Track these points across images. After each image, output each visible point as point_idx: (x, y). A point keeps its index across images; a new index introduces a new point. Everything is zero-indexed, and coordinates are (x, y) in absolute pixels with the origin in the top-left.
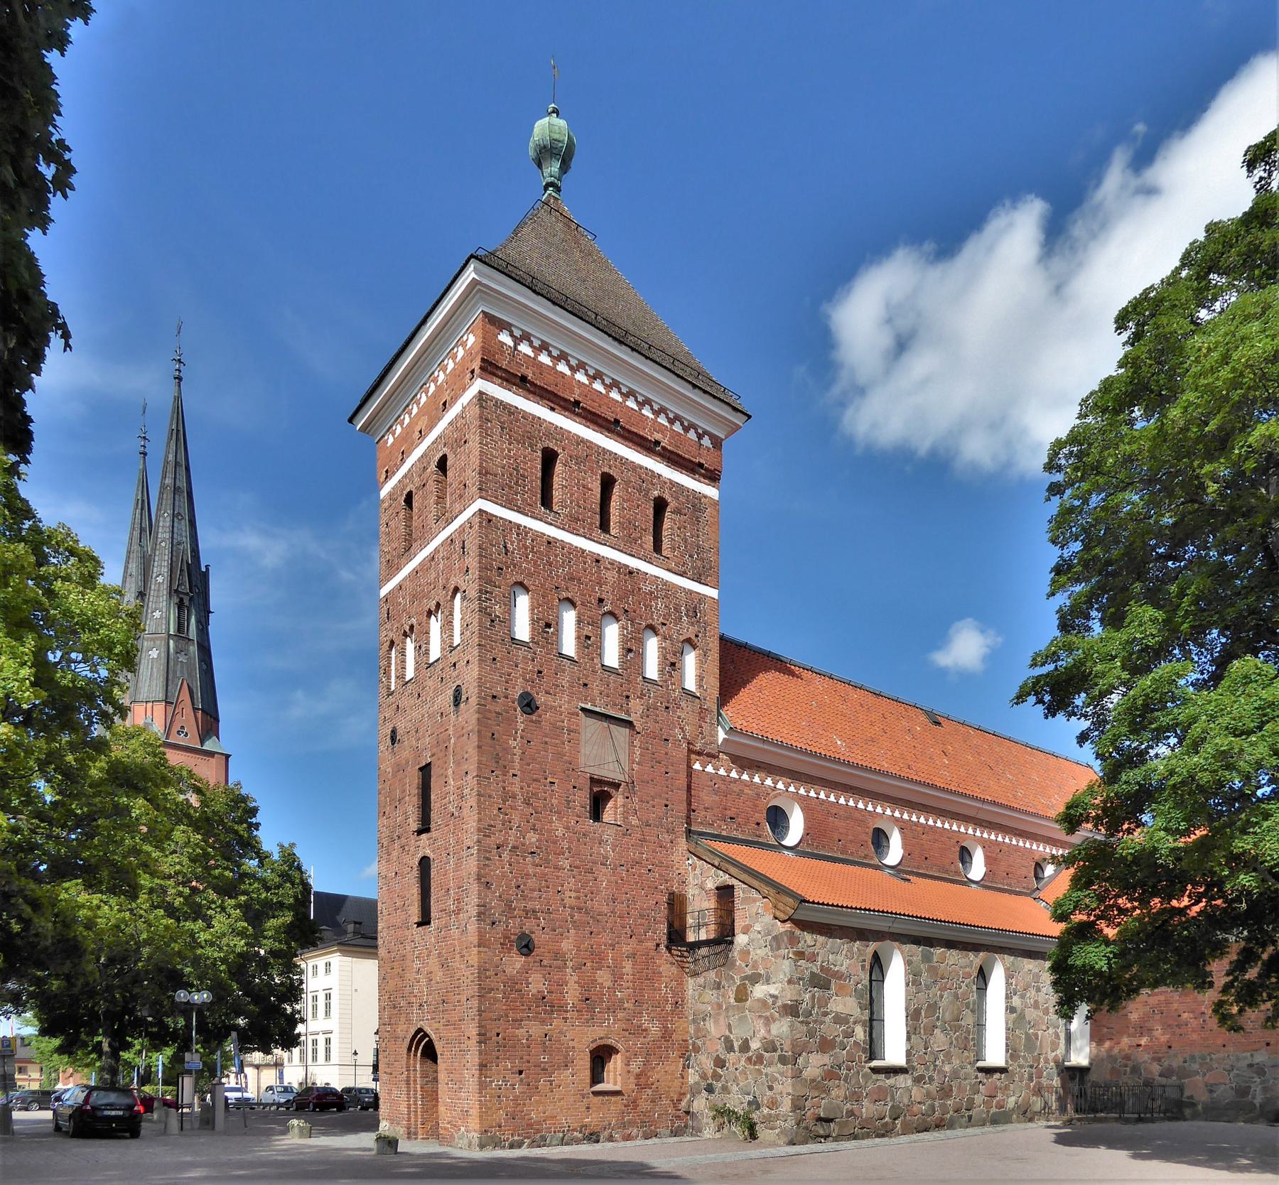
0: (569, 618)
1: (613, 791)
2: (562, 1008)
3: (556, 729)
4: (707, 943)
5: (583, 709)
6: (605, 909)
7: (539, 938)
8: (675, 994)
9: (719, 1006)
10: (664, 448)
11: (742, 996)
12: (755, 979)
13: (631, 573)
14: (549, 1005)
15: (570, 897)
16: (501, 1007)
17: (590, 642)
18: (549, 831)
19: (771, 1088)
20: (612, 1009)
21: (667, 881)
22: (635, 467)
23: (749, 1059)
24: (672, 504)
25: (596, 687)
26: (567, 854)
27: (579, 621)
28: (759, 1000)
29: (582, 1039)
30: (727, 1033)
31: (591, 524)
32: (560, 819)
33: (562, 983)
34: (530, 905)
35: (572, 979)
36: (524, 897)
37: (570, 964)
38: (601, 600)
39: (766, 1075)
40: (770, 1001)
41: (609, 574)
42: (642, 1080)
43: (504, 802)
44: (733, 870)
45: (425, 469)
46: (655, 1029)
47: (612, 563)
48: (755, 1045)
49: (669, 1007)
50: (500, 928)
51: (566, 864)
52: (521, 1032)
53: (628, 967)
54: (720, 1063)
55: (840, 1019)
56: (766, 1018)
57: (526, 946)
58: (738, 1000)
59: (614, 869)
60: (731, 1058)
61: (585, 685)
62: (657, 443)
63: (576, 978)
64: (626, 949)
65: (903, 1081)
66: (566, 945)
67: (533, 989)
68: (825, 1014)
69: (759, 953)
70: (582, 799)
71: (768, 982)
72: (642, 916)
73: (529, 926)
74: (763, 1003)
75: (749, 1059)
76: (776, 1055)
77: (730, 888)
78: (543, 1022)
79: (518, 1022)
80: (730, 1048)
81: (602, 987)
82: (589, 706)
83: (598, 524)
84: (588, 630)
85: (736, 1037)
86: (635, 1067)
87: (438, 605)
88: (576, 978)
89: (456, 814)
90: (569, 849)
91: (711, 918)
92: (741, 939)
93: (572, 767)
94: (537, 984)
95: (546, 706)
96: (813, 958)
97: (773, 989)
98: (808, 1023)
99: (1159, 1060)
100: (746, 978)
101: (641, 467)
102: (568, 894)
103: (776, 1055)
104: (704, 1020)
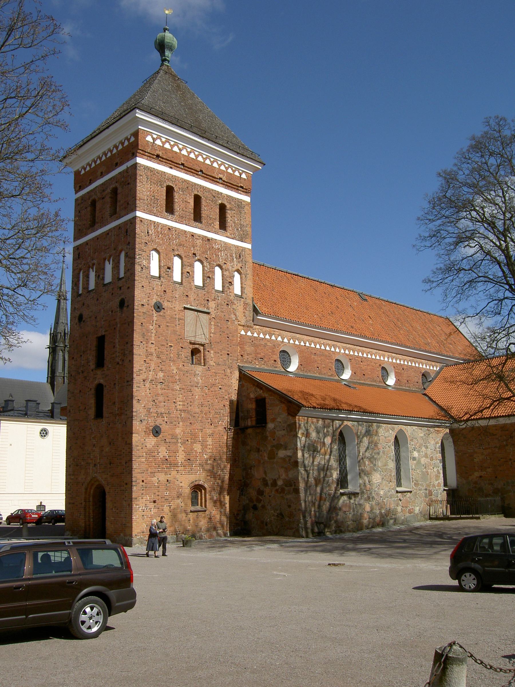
0: (177, 262)
1: (201, 348)
2: (176, 465)
4: (252, 427)
5: (185, 308)
6: (197, 410)
7: (164, 427)
10: (224, 181)
11: (272, 456)
12: (279, 447)
13: (209, 240)
14: (169, 463)
16: (144, 466)
18: (169, 371)
23: (277, 490)
24: (228, 206)
25: (192, 297)
26: (178, 382)
28: (281, 458)
30: (264, 476)
31: (189, 219)
32: (174, 364)
35: (181, 449)
36: (157, 406)
37: (180, 441)
38: (194, 254)
39: (287, 499)
40: (287, 459)
41: (198, 241)
43: (147, 357)
45: (104, 191)
47: (199, 236)
48: (280, 483)
50: (144, 423)
53: (210, 441)
56: (286, 468)
57: (156, 432)
58: (269, 458)
60: (267, 490)
61: (187, 296)
62: (220, 179)
63: (183, 449)
64: (209, 431)
66: (178, 431)
67: (161, 455)
71: (286, 448)
73: (159, 421)
74: (284, 459)
75: (277, 490)
76: (292, 488)
78: (166, 474)
82: (188, 306)
83: (192, 218)
84: (188, 269)
85: (270, 478)
88: (183, 449)
89: (121, 363)
91: (253, 414)
92: (270, 426)
93: (182, 338)
94: (163, 452)
95: (167, 308)
100: (274, 446)
101: (213, 190)
102: (179, 403)
103: (292, 488)
104: (251, 469)
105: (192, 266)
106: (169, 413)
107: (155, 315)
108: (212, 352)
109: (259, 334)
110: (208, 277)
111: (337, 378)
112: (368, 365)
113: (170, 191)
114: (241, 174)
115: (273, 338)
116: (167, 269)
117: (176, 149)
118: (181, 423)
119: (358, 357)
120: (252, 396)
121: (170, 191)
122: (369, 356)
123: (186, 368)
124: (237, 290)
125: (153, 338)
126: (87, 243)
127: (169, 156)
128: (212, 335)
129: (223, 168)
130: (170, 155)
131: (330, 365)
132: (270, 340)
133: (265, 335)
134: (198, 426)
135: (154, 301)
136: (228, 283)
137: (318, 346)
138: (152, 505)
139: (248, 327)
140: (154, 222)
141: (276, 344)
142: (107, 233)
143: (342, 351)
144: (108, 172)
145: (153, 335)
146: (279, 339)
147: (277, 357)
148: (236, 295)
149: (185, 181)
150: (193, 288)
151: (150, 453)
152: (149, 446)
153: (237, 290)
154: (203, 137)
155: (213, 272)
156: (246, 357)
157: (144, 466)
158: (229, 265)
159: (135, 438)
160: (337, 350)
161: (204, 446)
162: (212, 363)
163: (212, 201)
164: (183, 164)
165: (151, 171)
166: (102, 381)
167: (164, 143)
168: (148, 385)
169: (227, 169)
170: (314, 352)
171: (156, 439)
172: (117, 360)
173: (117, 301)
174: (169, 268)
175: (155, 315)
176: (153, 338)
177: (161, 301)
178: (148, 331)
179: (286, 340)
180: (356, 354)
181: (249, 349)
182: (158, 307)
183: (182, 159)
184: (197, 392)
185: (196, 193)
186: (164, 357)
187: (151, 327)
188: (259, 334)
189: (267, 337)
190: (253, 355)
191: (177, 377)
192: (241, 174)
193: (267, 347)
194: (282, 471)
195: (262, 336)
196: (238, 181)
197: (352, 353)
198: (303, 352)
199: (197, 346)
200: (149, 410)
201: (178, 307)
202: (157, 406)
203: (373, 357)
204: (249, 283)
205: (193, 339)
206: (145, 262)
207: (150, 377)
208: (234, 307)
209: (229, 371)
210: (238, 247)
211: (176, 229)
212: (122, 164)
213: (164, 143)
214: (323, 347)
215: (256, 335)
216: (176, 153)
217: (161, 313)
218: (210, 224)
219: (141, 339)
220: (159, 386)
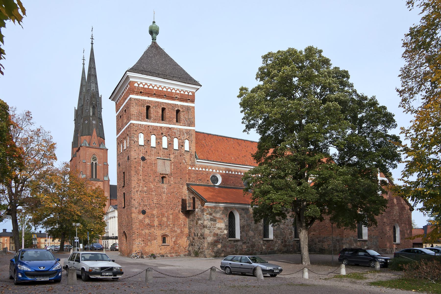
1: (167, 176)
2: (153, 226)
3: (151, 164)
6: (164, 203)
7: (147, 211)
8: (184, 222)
11: (197, 223)
12: (199, 219)
14: (150, 226)
15: (155, 201)
16: (138, 227)
17: (159, 143)
20: (167, 226)
22: (170, 104)
25: (161, 153)
32: (152, 184)
35: (156, 220)
42: (176, 243)
46: (179, 231)
48: (199, 235)
49: (182, 226)
50: (138, 209)
52: (143, 232)
53: (171, 217)
54: (194, 239)
57: (144, 212)
59: (167, 194)
65: (239, 243)
66: (155, 212)
69: (199, 213)
70: (159, 178)
73: (145, 208)
78: (149, 230)
79: (142, 230)
82: (159, 158)
86: (173, 240)
92: (197, 210)
93: (155, 172)
94: (147, 221)
99: (318, 238)
105: (161, 139)
109: (199, 169)
110: (170, 144)
114: (188, 93)
115: (207, 170)
118: (156, 209)
120: (191, 197)
121: (148, 108)
123: (158, 185)
132: (205, 171)
134: (164, 210)
135: (141, 156)
136: (181, 145)
138: (142, 242)
141: (208, 173)
145: (141, 171)
148: (186, 151)
150: (162, 149)
151: (141, 222)
155: (173, 141)
157: (138, 227)
158: (182, 137)
159: (133, 215)
161: (168, 219)
162: (172, 183)
168: (139, 193)
174: (148, 141)
178: (138, 170)
179: (214, 171)
181: (193, 175)
182: (143, 159)
184: (164, 196)
185: (163, 107)
186: (147, 181)
187: (140, 168)
188: (199, 169)
189: (204, 169)
191: (154, 189)
192: (188, 93)
195: (200, 169)
198: (222, 175)
199: (164, 176)
200: (140, 204)
202: (144, 202)
204: (194, 144)
205: (162, 172)
208: (184, 156)
209: (181, 186)
215: (197, 169)
217: (145, 162)
220: (145, 193)
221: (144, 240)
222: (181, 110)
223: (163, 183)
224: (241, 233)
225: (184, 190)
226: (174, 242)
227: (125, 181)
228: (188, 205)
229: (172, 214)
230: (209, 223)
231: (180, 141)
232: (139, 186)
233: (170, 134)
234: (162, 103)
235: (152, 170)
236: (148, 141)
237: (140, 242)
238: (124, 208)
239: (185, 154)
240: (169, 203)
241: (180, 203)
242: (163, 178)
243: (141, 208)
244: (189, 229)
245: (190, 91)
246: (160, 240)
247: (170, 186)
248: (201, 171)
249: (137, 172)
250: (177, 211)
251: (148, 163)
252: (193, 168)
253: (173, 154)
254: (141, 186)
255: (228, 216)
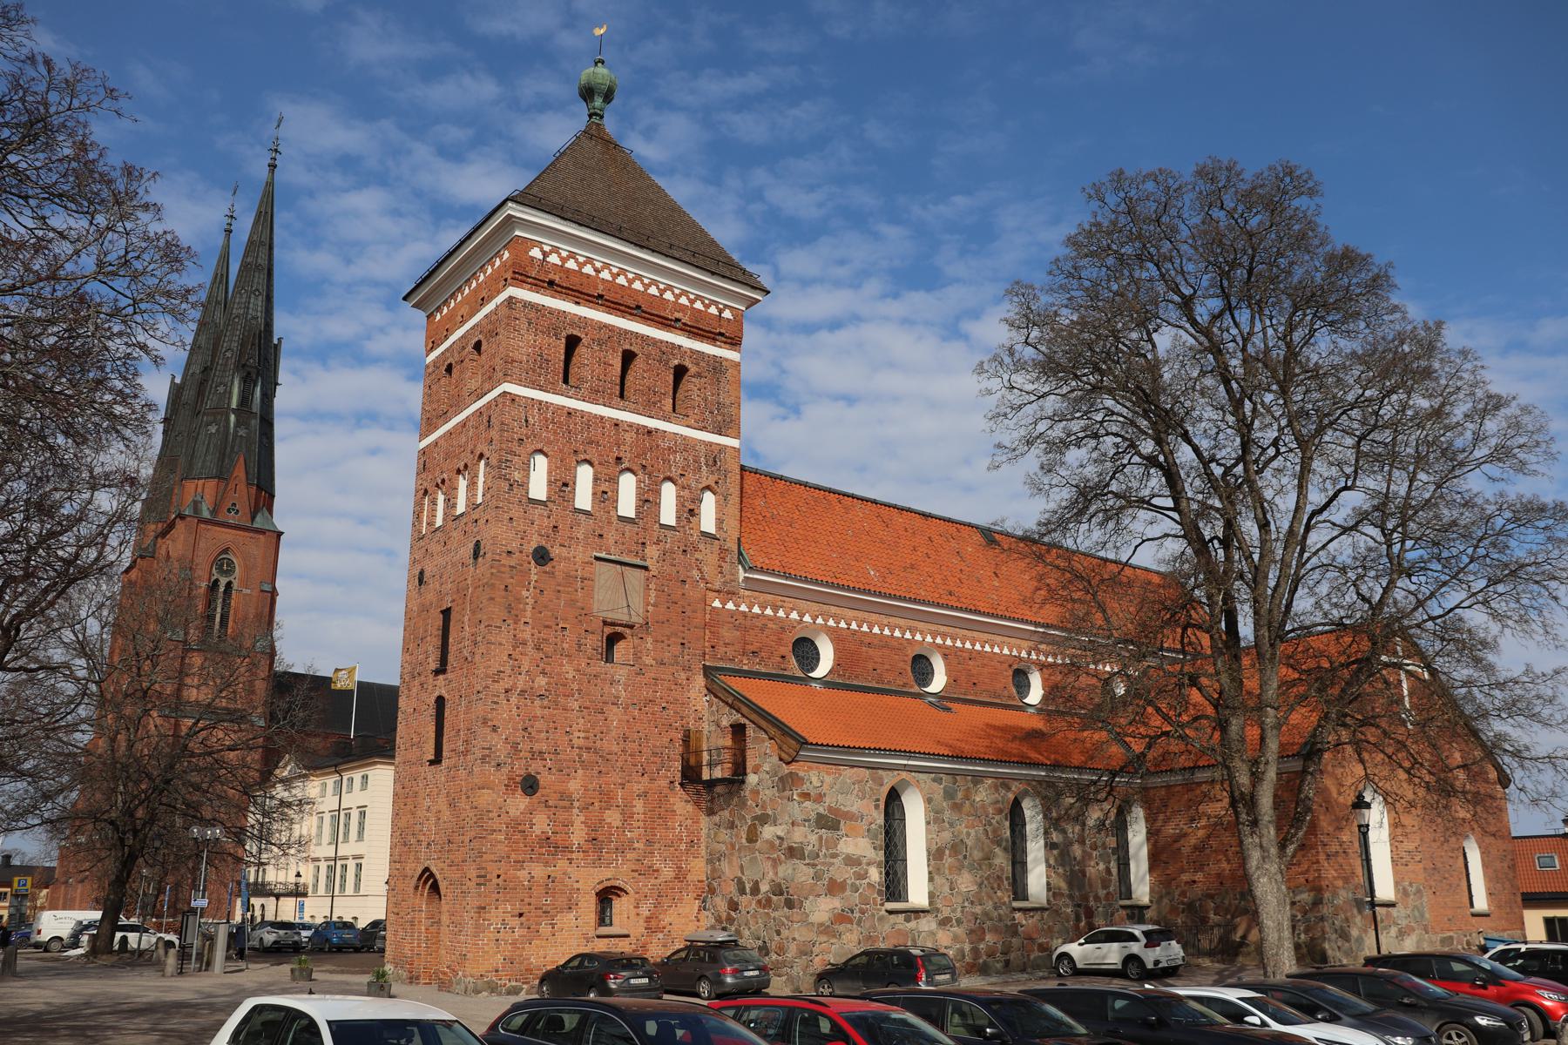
0: (585, 475)
2: (567, 849)
5: (597, 559)
6: (615, 748)
7: (545, 779)
8: (690, 833)
9: (733, 846)
11: (752, 837)
12: (763, 819)
13: (649, 432)
14: (553, 846)
16: (502, 849)
17: (605, 495)
19: (778, 933)
21: (682, 718)
27: (596, 479)
29: (588, 879)
32: (570, 662)
33: (567, 824)
34: (537, 747)
35: (578, 819)
36: (531, 738)
37: (576, 804)
38: (618, 459)
41: (627, 436)
42: (653, 923)
44: (745, 710)
46: (667, 872)
47: (631, 425)
48: (764, 888)
49: (683, 847)
50: (505, 770)
51: (576, 705)
52: (523, 874)
53: (639, 806)
54: (734, 906)
55: (851, 861)
56: (774, 860)
57: (530, 785)
61: (601, 536)
62: (677, 320)
64: (637, 788)
66: (574, 786)
67: (537, 830)
68: (834, 856)
69: (767, 794)
70: (595, 642)
72: (655, 754)
75: (759, 902)
76: (782, 898)
77: (743, 726)
78: (547, 864)
79: (520, 863)
80: (742, 891)
81: (610, 827)
82: (603, 555)
86: (645, 911)
87: (466, 466)
90: (579, 690)
92: (752, 779)
93: (585, 613)
96: (819, 798)
97: (780, 830)
98: (814, 865)
102: (577, 734)
103: (782, 898)
105: (614, 481)
106: (556, 753)
107: (534, 571)
108: (650, 640)
109: (750, 607)
110: (648, 501)
111: (916, 689)
112: (984, 666)
113: (572, 343)
114: (721, 311)
115: (781, 613)
116: (562, 486)
117: (588, 269)
118: (580, 772)
119: (963, 650)
120: (725, 722)
121: (572, 343)
122: (987, 648)
124: (708, 522)
125: (528, 614)
126: (436, 443)
127: (574, 282)
128: (650, 608)
129: (683, 300)
130: (575, 280)
131: (901, 664)
132: (774, 619)
133: (763, 608)
134: (615, 777)
135: (534, 545)
136: (689, 512)
137: (876, 630)
138: (516, 922)
139: (728, 593)
140: (540, 402)
141: (784, 626)
142: (464, 424)
143: (929, 639)
144: (472, 315)
145: (529, 608)
146: (794, 615)
147: (787, 650)
148: (704, 534)
149: (606, 326)
152: (513, 812)
153: (708, 522)
154: (642, 247)
155: (658, 493)
156: (721, 650)
157: (502, 849)
158: (691, 479)
160: (918, 637)
161: (627, 817)
162: (648, 661)
163: (660, 361)
164: (600, 296)
165: (538, 311)
166: (444, 693)
167: (564, 260)
168: (514, 700)
169: (692, 302)
170: (867, 640)
171: (528, 799)
172: (466, 653)
173: (471, 546)
174: (565, 485)
175: (534, 571)
176: (528, 614)
177: (548, 547)
178: (519, 600)
179: (807, 618)
180: (959, 644)
181: (727, 634)
182: (542, 556)
183: (601, 287)
184: (615, 715)
185: (627, 347)
186: (549, 649)
187: (525, 593)
188: (750, 608)
189: (769, 612)
190: (738, 647)
192: (721, 311)
193: (767, 632)
194: (767, 866)
195: (756, 610)
196: (715, 324)
197: (949, 642)
198: (837, 637)
199: (619, 629)
200: (515, 746)
201: (581, 554)
202: (531, 738)
203: (996, 650)
204: (733, 509)
205: (611, 616)
206: (517, 476)
207: (520, 685)
209: (683, 675)
210: (711, 444)
211: (583, 414)
212: (491, 298)
213: (564, 260)
214: (887, 632)
215: (743, 608)
216: (588, 276)
217: (547, 568)
218: (655, 403)
219: (504, 615)
220: (538, 702)
221: (525, 910)
222: (693, 369)
223: (609, 658)
224: (931, 879)
225: (692, 694)
226: (648, 920)
227: (452, 649)
228: (706, 757)
229: (645, 794)
230: (813, 838)
231: (686, 493)
232: (517, 670)
233: (651, 459)
234: (626, 332)
235: (572, 603)
236: (565, 485)
237: (508, 918)
238: (437, 761)
239: (701, 546)
240: (635, 746)
241: (678, 745)
242: (613, 640)
243: (520, 770)
244: (710, 861)
245: (726, 306)
246: (589, 905)
247: (640, 673)
248: (758, 616)
249: (512, 612)
250: (664, 783)
251: (560, 576)
252: (730, 606)
253: (658, 542)
254: (524, 669)
255: (882, 806)
